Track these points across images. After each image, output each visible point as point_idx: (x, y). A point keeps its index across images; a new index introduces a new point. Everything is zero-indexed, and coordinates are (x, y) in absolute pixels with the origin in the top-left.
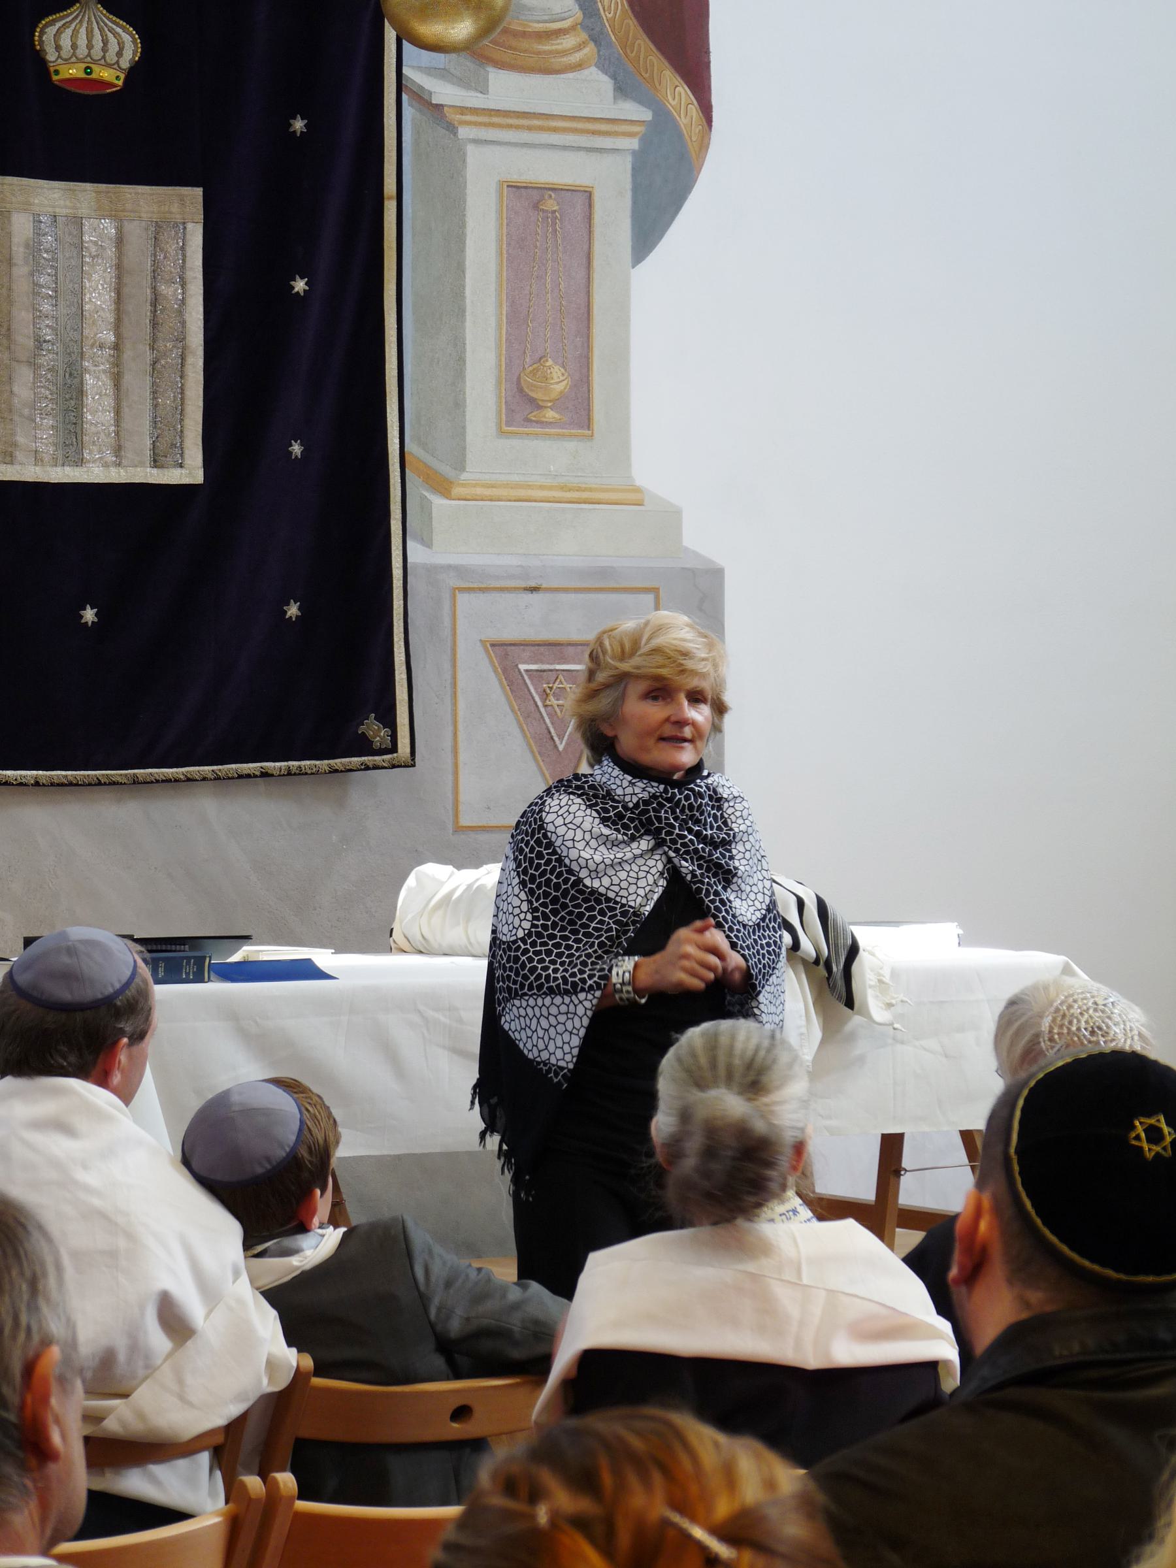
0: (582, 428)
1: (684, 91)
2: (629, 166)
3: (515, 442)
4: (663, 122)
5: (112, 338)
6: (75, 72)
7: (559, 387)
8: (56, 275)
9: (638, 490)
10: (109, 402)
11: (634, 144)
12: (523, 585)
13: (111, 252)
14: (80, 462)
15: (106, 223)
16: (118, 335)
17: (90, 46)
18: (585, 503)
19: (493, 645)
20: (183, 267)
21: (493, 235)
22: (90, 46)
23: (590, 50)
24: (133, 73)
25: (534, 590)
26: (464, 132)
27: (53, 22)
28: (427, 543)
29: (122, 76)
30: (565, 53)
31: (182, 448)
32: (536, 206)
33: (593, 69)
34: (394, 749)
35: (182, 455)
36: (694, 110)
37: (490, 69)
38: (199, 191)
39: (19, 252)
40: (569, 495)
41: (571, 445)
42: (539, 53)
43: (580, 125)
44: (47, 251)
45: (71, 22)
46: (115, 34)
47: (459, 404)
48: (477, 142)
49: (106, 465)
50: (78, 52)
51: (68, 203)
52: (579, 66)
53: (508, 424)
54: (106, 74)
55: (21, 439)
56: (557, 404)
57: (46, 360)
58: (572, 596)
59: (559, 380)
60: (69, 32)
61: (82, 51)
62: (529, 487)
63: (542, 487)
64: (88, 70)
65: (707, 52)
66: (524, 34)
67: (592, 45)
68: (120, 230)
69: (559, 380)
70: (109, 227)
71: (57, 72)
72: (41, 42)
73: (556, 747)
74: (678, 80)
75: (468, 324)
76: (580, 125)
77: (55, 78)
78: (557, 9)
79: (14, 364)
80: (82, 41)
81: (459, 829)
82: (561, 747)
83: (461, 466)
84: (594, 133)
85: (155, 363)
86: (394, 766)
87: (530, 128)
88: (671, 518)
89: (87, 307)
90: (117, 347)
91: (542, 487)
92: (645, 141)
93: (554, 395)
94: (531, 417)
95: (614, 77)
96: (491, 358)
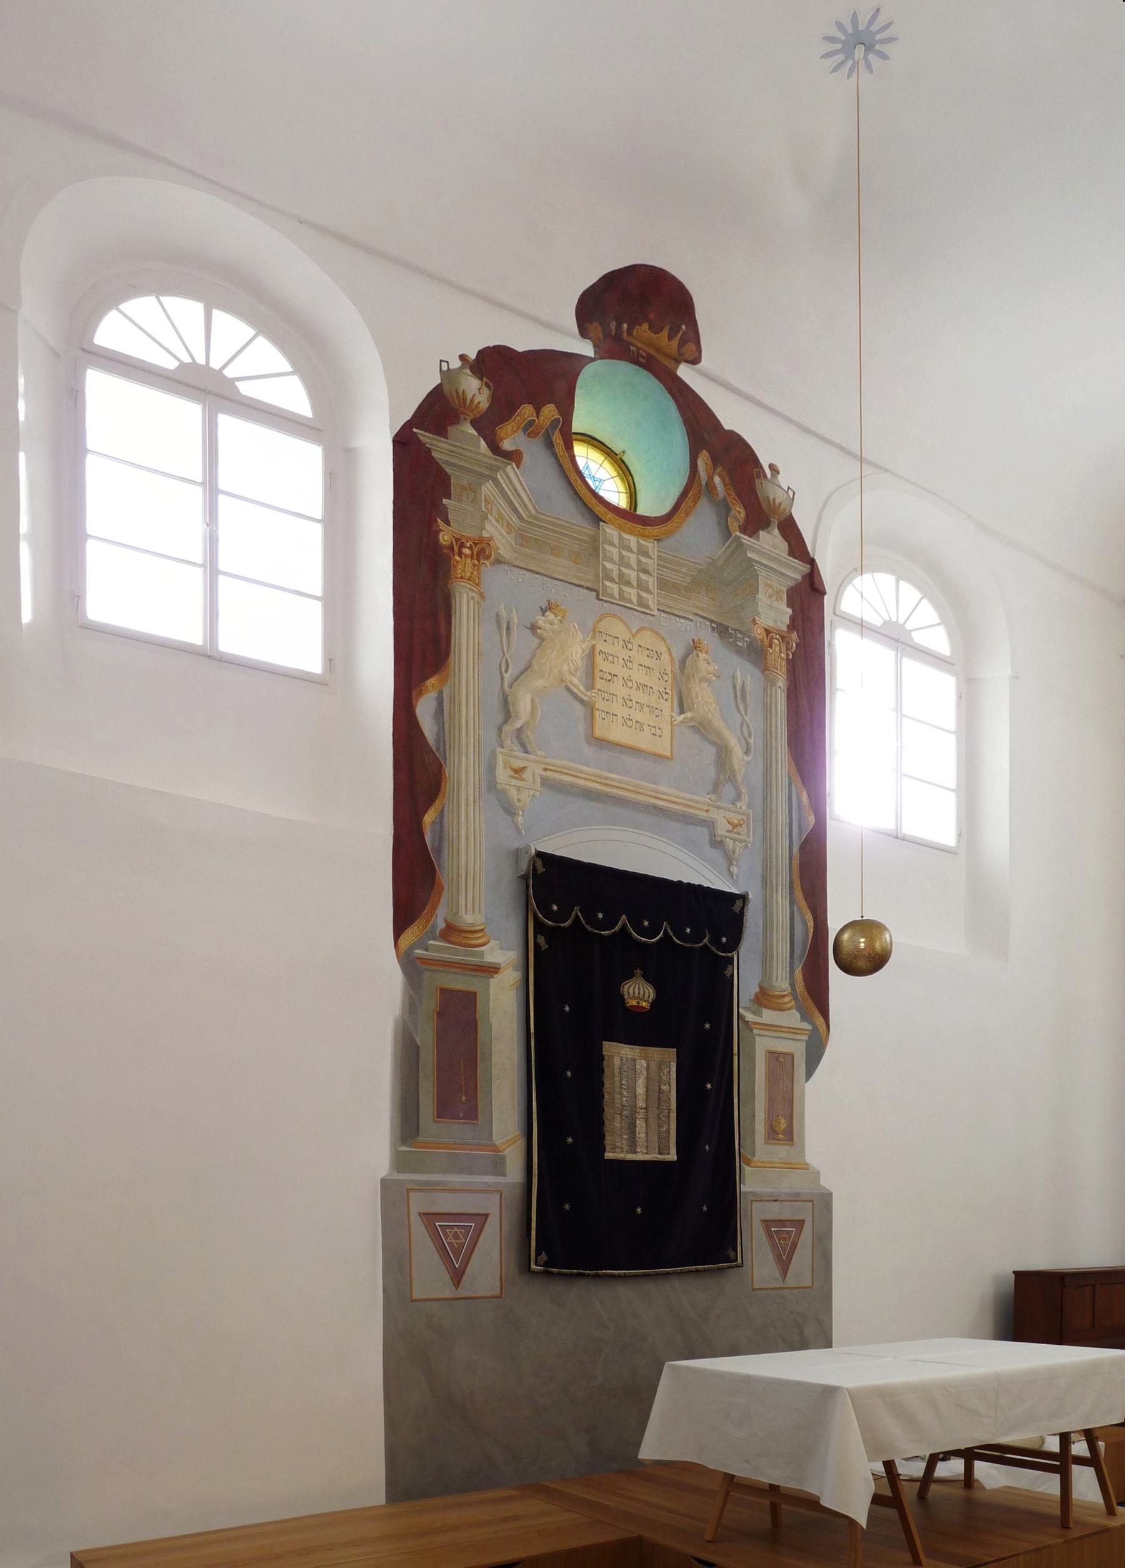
0: (790, 1141)
1: (821, 1019)
2: (805, 1046)
3: (770, 1146)
4: (815, 1029)
5: (644, 1105)
6: (634, 1003)
7: (783, 1126)
8: (628, 1081)
9: (807, 1164)
10: (644, 1130)
11: (806, 1038)
12: (772, 1199)
13: (645, 1073)
14: (636, 1152)
15: (643, 1061)
16: (646, 1104)
17: (639, 993)
18: (792, 1168)
19: (764, 1221)
20: (669, 1079)
21: (763, 1070)
22: (639, 993)
23: (793, 1002)
24: (652, 1004)
25: (776, 1201)
26: (755, 1031)
27: (626, 984)
28: (744, 1184)
29: (649, 1005)
30: (785, 1003)
31: (669, 1147)
32: (777, 1060)
33: (794, 1010)
34: (737, 1261)
35: (669, 1150)
36: (824, 1026)
37: (763, 1008)
38: (675, 1050)
39: (617, 1071)
40: (787, 1166)
41: (787, 1147)
42: (778, 1003)
43: (790, 1030)
44: (625, 1072)
45: (633, 984)
46: (647, 989)
47: (753, 1132)
48: (759, 1035)
49: (643, 1153)
50: (640, 995)
51: (632, 1054)
52: (790, 1009)
53: (768, 1140)
54: (644, 1004)
55: (617, 1144)
56: (783, 1132)
57: (625, 1113)
58: (787, 1203)
59: (783, 1124)
60: (632, 987)
61: (637, 995)
62: (774, 1163)
63: (778, 1163)
64: (638, 1003)
65: (828, 1005)
66: (774, 996)
67: (794, 1001)
68: (648, 1064)
69: (783, 1124)
70: (644, 1063)
71: (628, 1003)
72: (623, 991)
73: (455, 1266)
74: (819, 1015)
75: (756, 1103)
76: (790, 1030)
77: (627, 1005)
78: (783, 987)
79: (615, 1115)
80: (637, 992)
81: (753, 1289)
82: (457, 1267)
83: (753, 1155)
84: (794, 1033)
85: (659, 1115)
86: (737, 1267)
87: (775, 1031)
88: (817, 1174)
89: (637, 1093)
90: (646, 1108)
91: (778, 1163)
92: (810, 1037)
93: (782, 1129)
94: (775, 1137)
95: (800, 1013)
96: (763, 1115)
